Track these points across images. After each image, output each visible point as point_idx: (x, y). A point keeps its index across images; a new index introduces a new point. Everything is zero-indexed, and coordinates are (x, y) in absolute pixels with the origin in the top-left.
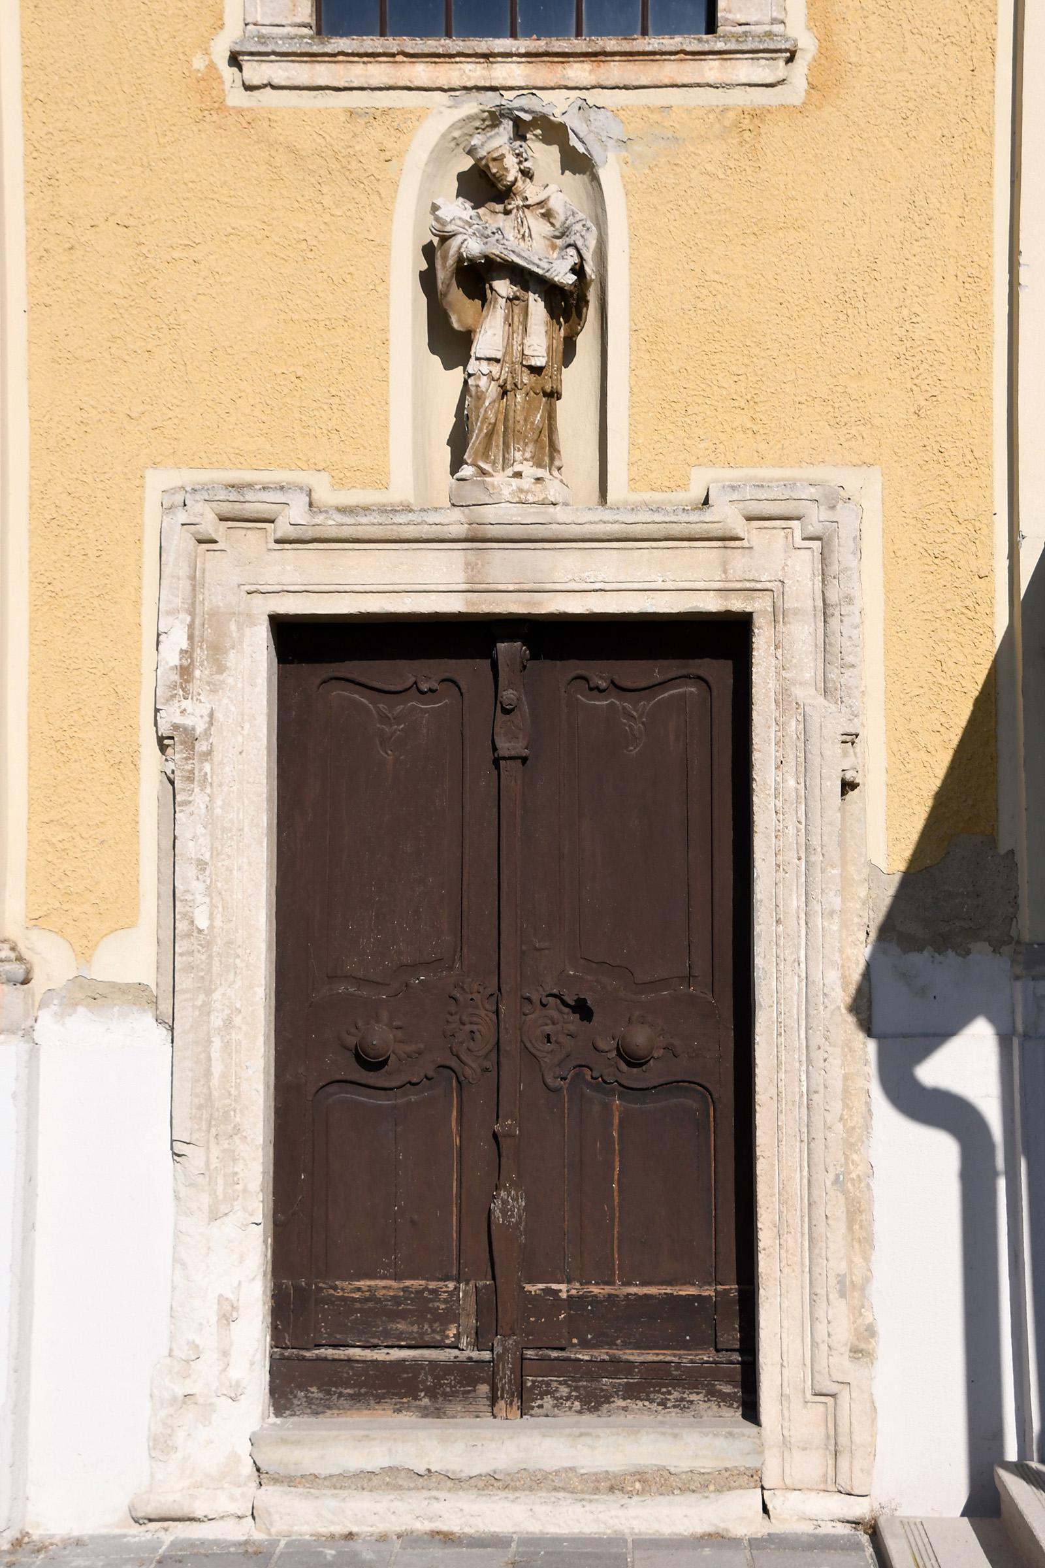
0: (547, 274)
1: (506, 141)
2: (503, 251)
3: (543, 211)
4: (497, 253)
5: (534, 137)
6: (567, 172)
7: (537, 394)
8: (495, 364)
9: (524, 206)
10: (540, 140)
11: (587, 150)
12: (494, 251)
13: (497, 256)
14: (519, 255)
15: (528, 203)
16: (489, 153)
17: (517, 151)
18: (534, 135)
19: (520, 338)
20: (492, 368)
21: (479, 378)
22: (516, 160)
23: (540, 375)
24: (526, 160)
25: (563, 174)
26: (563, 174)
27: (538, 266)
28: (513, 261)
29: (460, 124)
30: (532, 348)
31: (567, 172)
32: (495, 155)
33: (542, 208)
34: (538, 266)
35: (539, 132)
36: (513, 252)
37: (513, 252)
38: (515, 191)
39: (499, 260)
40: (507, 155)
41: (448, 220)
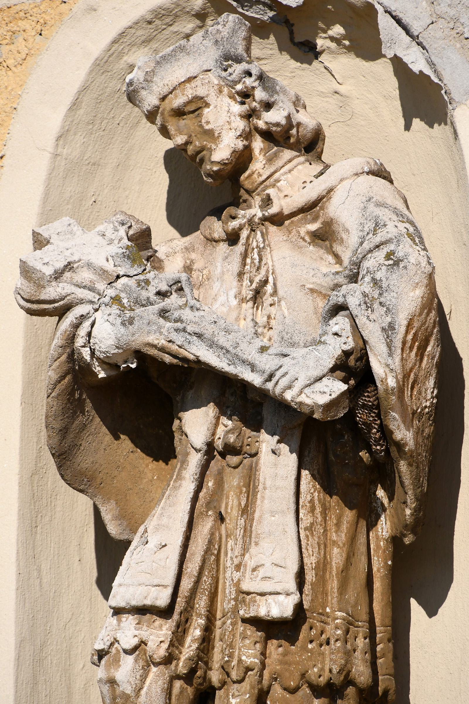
0: (269, 386)
1: (210, 64)
2: (174, 336)
3: (314, 227)
4: (162, 342)
5: (333, 45)
6: (417, 123)
7: (293, 691)
8: (159, 621)
9: (265, 219)
10: (349, 49)
11: (431, 64)
12: (152, 339)
13: (162, 350)
14: (212, 344)
15: (273, 210)
16: (163, 99)
17: (239, 87)
18: (332, 39)
19: (238, 550)
20: (144, 634)
21: (116, 662)
22: (237, 108)
23: (292, 639)
24: (268, 106)
25: (408, 127)
26: (408, 127)
27: (253, 368)
28: (198, 362)
29: (142, 33)
30: (261, 572)
31: (417, 123)
32: (178, 101)
33: (315, 219)
34: (253, 368)
35: (338, 30)
36: (199, 336)
37: (199, 336)
38: (248, 185)
39: (168, 359)
40: (212, 99)
41: (48, 271)
